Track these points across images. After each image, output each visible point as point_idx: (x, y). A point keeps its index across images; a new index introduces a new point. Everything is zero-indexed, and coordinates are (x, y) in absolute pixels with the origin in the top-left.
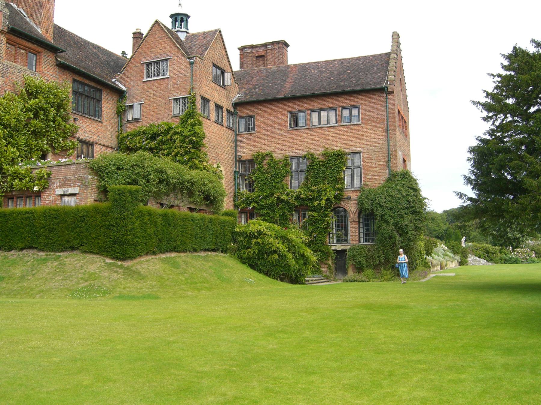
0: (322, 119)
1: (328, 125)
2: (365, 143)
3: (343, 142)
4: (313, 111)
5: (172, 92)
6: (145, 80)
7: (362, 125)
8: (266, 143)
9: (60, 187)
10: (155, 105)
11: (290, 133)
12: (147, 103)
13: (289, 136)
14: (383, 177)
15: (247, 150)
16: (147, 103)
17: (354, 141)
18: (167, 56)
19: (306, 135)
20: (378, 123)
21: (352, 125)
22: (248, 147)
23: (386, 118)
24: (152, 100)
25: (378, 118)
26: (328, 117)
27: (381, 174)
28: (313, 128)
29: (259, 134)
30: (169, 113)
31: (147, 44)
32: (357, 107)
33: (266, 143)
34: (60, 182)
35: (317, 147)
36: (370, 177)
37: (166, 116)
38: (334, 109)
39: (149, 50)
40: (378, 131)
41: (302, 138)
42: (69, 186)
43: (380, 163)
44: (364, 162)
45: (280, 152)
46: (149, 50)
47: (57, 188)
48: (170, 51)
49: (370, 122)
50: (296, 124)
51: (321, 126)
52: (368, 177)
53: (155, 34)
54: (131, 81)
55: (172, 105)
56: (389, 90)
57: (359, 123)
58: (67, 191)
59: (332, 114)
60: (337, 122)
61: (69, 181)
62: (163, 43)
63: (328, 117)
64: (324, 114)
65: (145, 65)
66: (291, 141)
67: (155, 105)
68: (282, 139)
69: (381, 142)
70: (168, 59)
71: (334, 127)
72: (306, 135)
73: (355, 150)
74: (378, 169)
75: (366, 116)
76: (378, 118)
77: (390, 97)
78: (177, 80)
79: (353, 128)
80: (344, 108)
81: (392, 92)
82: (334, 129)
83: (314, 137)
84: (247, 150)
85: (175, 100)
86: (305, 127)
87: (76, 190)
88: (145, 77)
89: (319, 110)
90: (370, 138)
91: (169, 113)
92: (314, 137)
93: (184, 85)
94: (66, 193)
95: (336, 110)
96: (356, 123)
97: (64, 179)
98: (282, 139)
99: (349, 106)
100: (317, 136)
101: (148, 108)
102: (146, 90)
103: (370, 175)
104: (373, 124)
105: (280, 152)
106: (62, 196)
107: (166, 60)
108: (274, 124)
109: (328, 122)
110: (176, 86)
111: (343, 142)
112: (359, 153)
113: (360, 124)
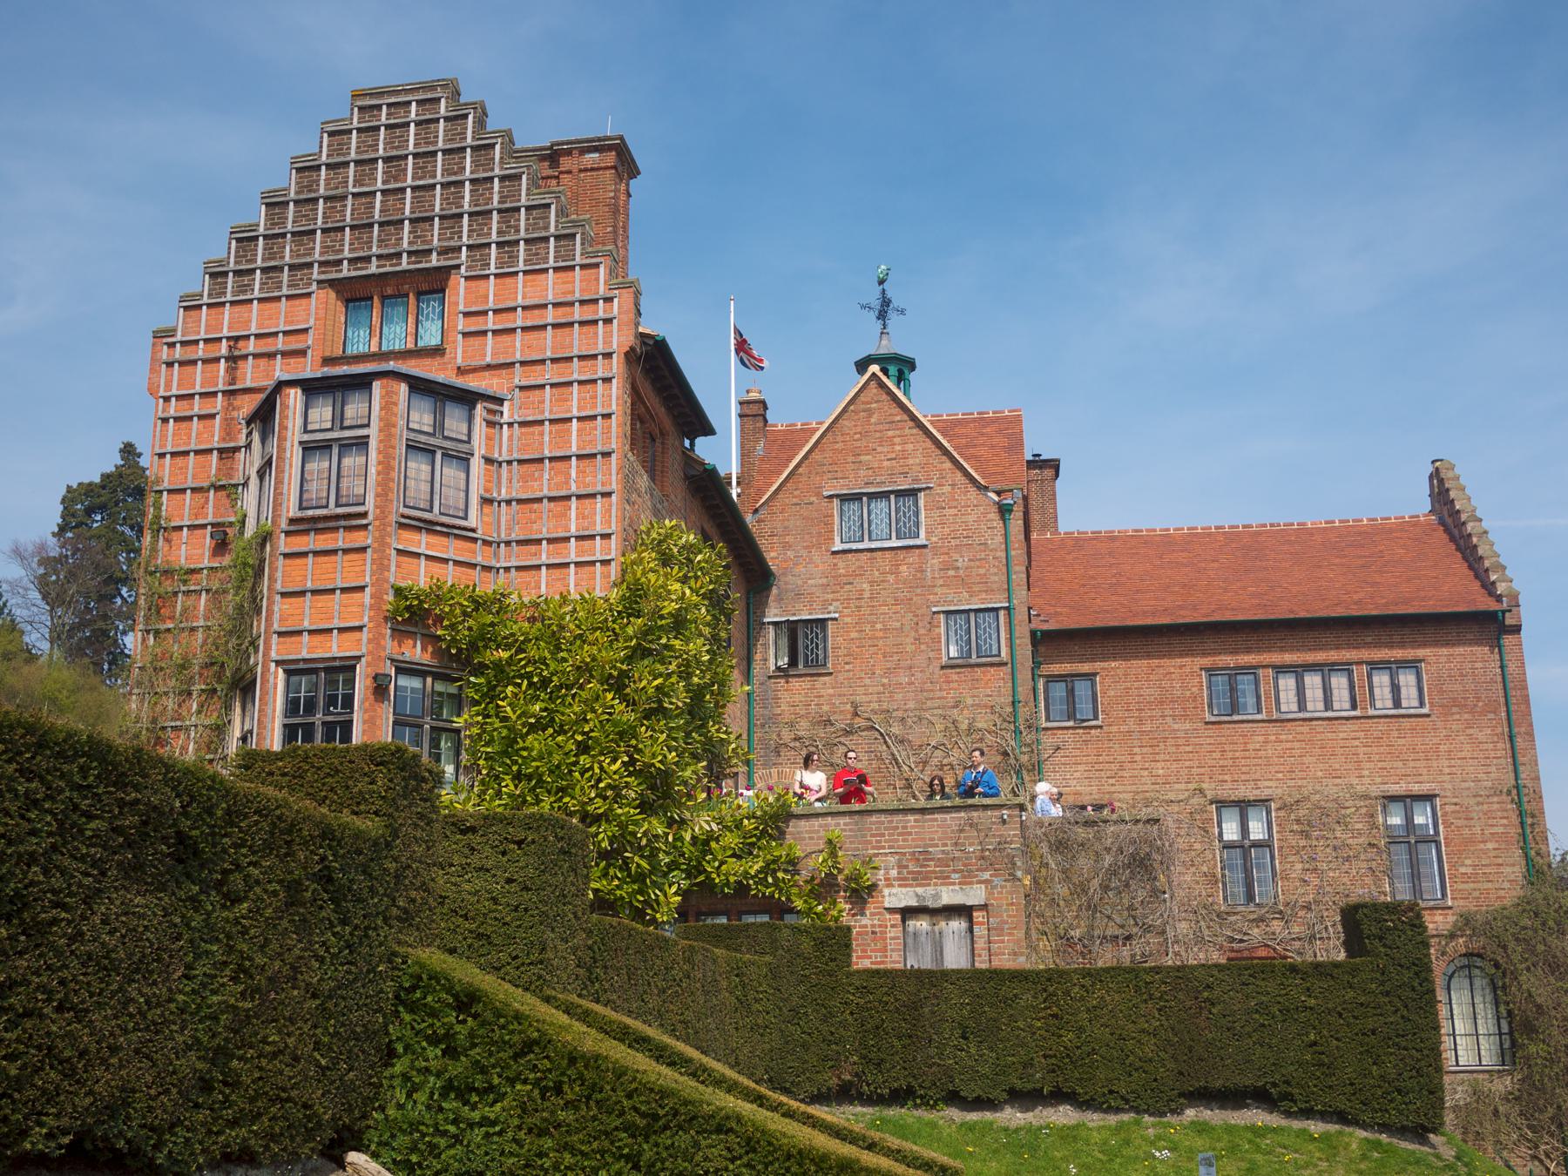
0: (1308, 693)
1: (1301, 715)
2: (1447, 770)
3: (1380, 765)
4: (1281, 669)
5: (938, 590)
6: (838, 546)
7: (1433, 718)
8: (1138, 758)
9: (903, 881)
10: (879, 626)
11: (1212, 731)
12: (848, 620)
13: (1209, 741)
14: (1509, 869)
15: (1077, 775)
16: (848, 620)
17: (1412, 764)
18: (916, 480)
19: (1261, 739)
20: (1482, 713)
21: (1403, 716)
22: (1081, 768)
23: (1502, 700)
24: (865, 611)
25: (1479, 699)
26: (1395, 689)
27: (1500, 861)
28: (1283, 721)
29: (1114, 729)
30: (931, 655)
31: (839, 438)
32: (1413, 665)
33: (1138, 758)
34: (900, 867)
35: (1300, 774)
36: (1469, 870)
37: (921, 660)
38: (1345, 668)
39: (850, 459)
40: (1481, 736)
41: (1250, 747)
42: (945, 879)
43: (1495, 830)
44: (1447, 825)
45: (1183, 786)
46: (850, 459)
47: (890, 885)
48: (923, 466)
49: (1455, 710)
50: (1235, 708)
51: (1308, 715)
52: (1463, 870)
53: (870, 412)
54: (787, 546)
55: (943, 629)
56: (1508, 621)
57: (1425, 711)
58: (937, 896)
59: (1339, 682)
60: (1354, 707)
61: (942, 863)
62: (897, 440)
63: (1395, 689)
64: (1313, 681)
65: (836, 502)
66: (1217, 755)
67: (879, 626)
68: (1188, 749)
69: (1493, 769)
70: (920, 490)
71: (1347, 719)
72: (1261, 739)
73: (1416, 789)
74: (1490, 846)
75: (1441, 692)
76: (1479, 699)
77: (1508, 640)
78: (956, 556)
79: (1406, 723)
80: (1375, 666)
81: (1517, 629)
82: (1350, 726)
83: (1289, 745)
84: (1077, 775)
85: (947, 613)
86: (1259, 717)
87: (974, 895)
88: (837, 539)
89: (1299, 670)
90: (1460, 755)
91: (931, 655)
92: (1289, 745)
93: (982, 571)
94: (930, 904)
95: (1350, 673)
96: (1412, 711)
97: (922, 857)
98: (1188, 749)
99: (1389, 662)
100: (1297, 745)
101: (854, 635)
102: (844, 580)
103: (1468, 862)
104: (1466, 716)
105: (1183, 786)
106: (907, 913)
107: (913, 493)
108: (1162, 703)
109: (1328, 705)
110: (951, 573)
111: (1380, 765)
112: (1429, 798)
113: (1428, 716)
